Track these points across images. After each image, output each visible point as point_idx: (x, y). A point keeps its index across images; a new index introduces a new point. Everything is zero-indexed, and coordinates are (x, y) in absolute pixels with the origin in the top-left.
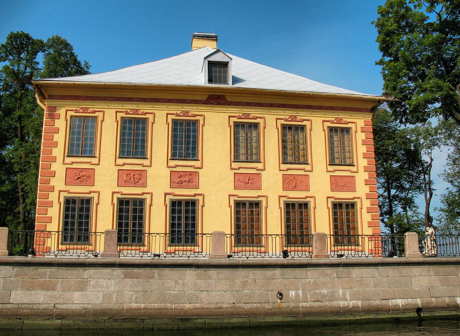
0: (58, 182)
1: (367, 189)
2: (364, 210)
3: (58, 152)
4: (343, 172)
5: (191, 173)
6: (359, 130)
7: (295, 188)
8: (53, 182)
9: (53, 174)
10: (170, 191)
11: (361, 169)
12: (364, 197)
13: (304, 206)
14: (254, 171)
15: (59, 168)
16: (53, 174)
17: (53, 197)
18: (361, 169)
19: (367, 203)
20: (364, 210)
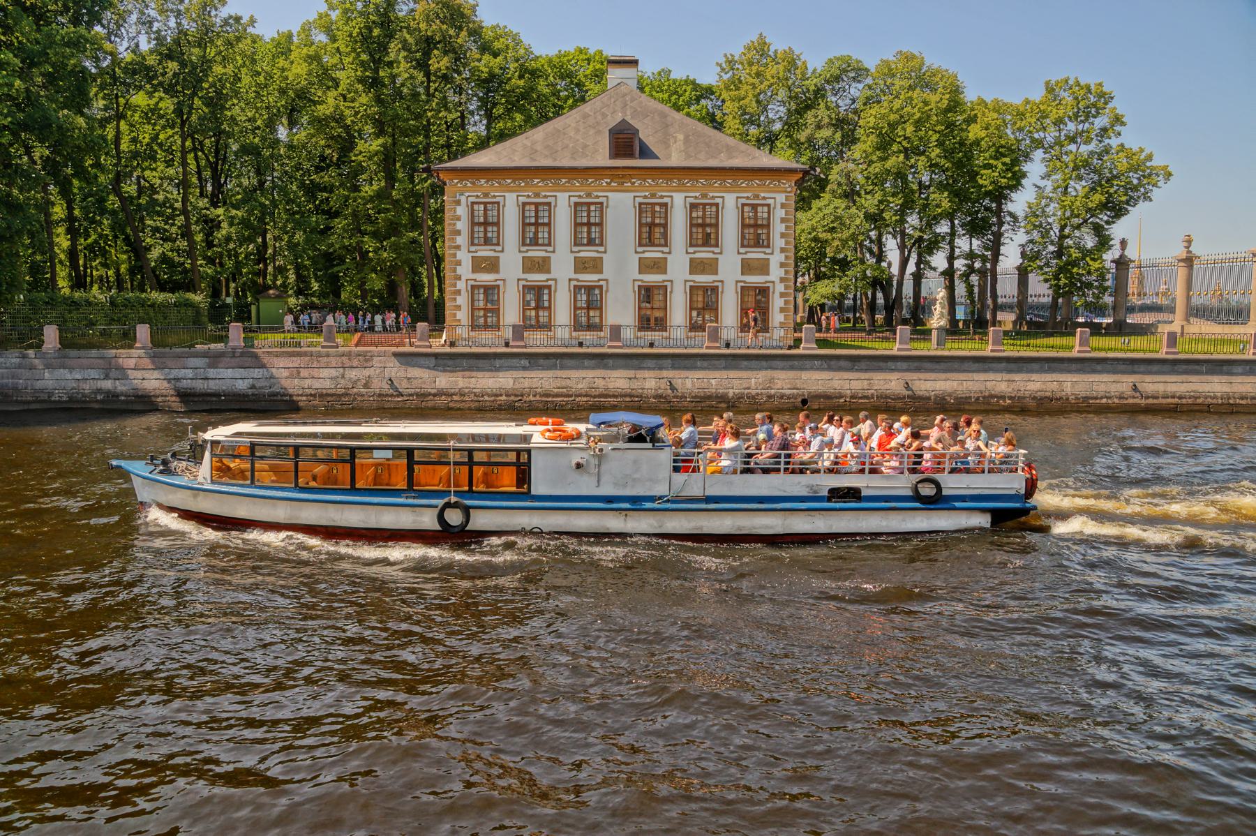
0: (465, 270)
1: (782, 273)
2: (777, 295)
3: (462, 240)
4: (755, 254)
5: (594, 259)
6: (779, 206)
7: (703, 272)
8: (459, 270)
9: (459, 263)
10: (574, 276)
11: (777, 251)
12: (777, 281)
13: (715, 290)
14: (660, 255)
15: (464, 256)
16: (459, 263)
17: (461, 285)
18: (777, 251)
19: (780, 288)
20: (777, 295)
